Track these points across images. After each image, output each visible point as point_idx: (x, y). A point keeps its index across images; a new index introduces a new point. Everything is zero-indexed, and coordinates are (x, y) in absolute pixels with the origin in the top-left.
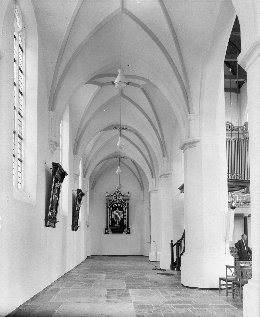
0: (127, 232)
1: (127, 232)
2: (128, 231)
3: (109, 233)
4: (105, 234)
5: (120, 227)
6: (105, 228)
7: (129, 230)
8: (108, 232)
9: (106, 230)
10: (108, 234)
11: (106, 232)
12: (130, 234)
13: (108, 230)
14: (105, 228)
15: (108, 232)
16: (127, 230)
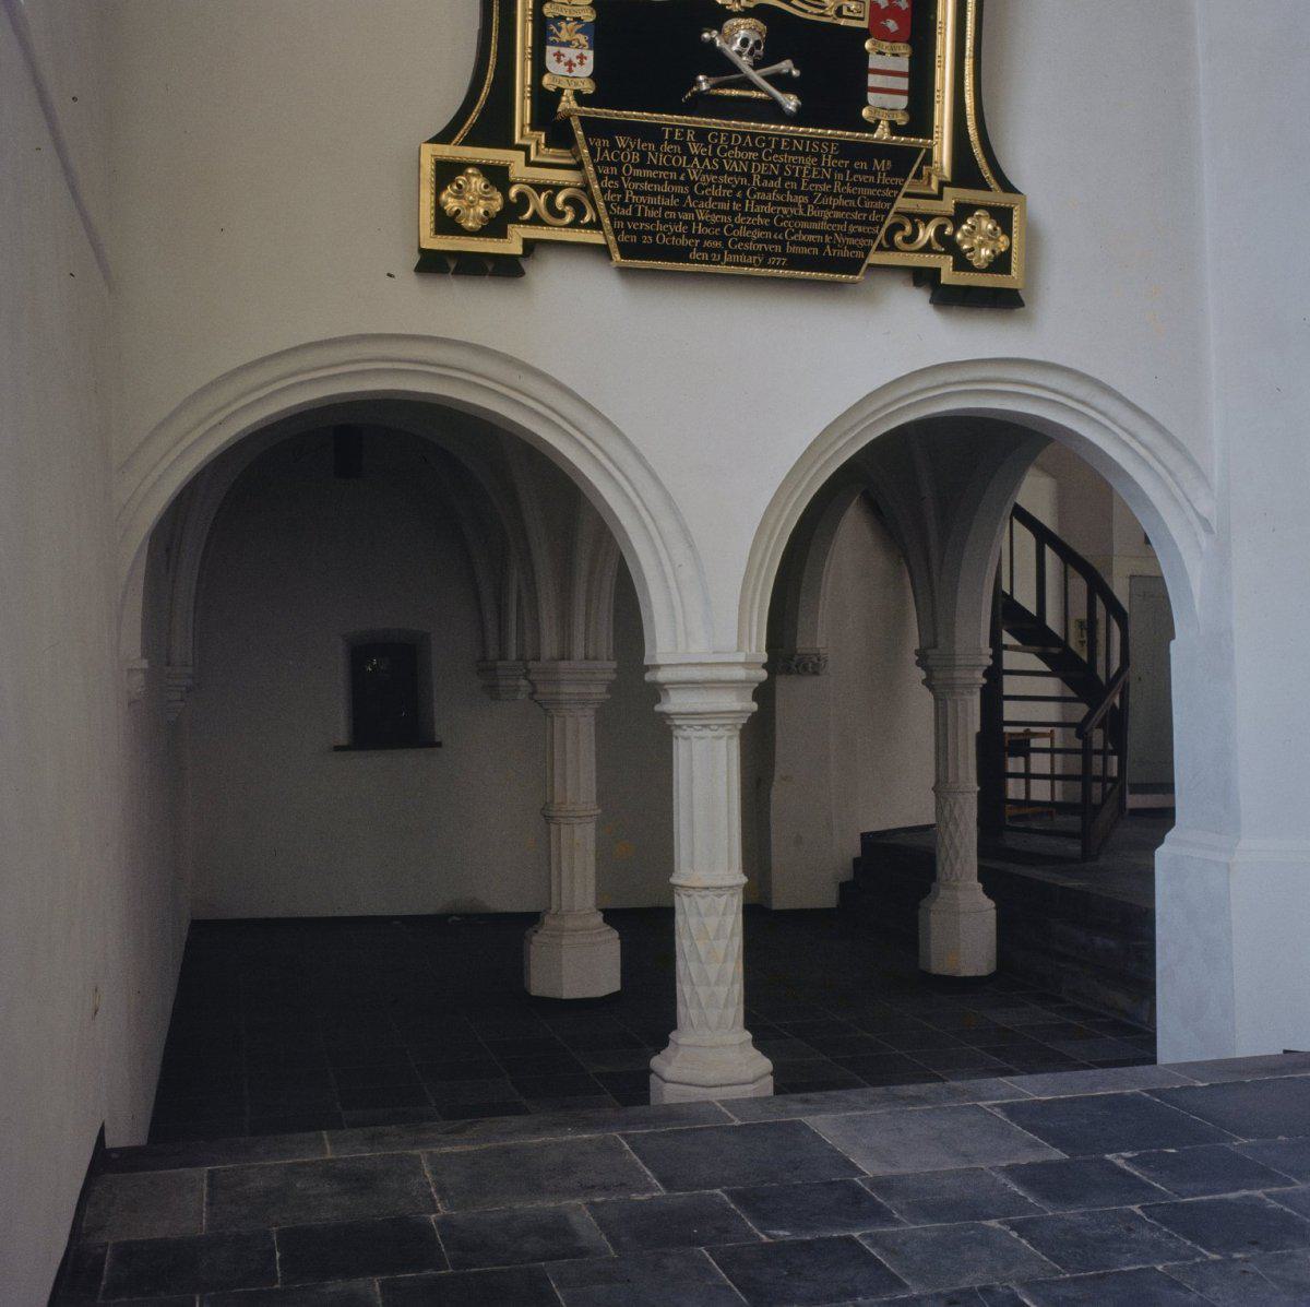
0: (963, 264)
1: (963, 264)
2: (980, 241)
3: (512, 245)
4: (431, 264)
5: (796, 119)
6: (444, 137)
7: (1003, 217)
8: (495, 227)
9: (447, 172)
10: (507, 269)
11: (446, 223)
12: (1005, 302)
13: (497, 176)
14: (444, 137)
15: (495, 227)
16: (963, 211)
